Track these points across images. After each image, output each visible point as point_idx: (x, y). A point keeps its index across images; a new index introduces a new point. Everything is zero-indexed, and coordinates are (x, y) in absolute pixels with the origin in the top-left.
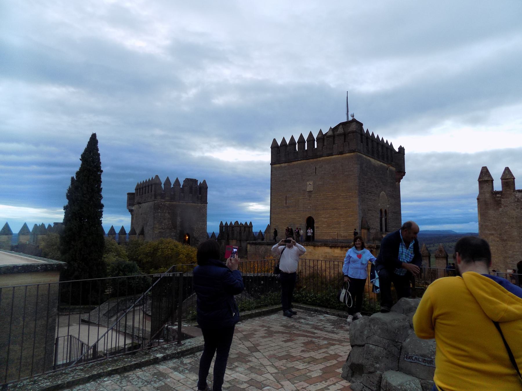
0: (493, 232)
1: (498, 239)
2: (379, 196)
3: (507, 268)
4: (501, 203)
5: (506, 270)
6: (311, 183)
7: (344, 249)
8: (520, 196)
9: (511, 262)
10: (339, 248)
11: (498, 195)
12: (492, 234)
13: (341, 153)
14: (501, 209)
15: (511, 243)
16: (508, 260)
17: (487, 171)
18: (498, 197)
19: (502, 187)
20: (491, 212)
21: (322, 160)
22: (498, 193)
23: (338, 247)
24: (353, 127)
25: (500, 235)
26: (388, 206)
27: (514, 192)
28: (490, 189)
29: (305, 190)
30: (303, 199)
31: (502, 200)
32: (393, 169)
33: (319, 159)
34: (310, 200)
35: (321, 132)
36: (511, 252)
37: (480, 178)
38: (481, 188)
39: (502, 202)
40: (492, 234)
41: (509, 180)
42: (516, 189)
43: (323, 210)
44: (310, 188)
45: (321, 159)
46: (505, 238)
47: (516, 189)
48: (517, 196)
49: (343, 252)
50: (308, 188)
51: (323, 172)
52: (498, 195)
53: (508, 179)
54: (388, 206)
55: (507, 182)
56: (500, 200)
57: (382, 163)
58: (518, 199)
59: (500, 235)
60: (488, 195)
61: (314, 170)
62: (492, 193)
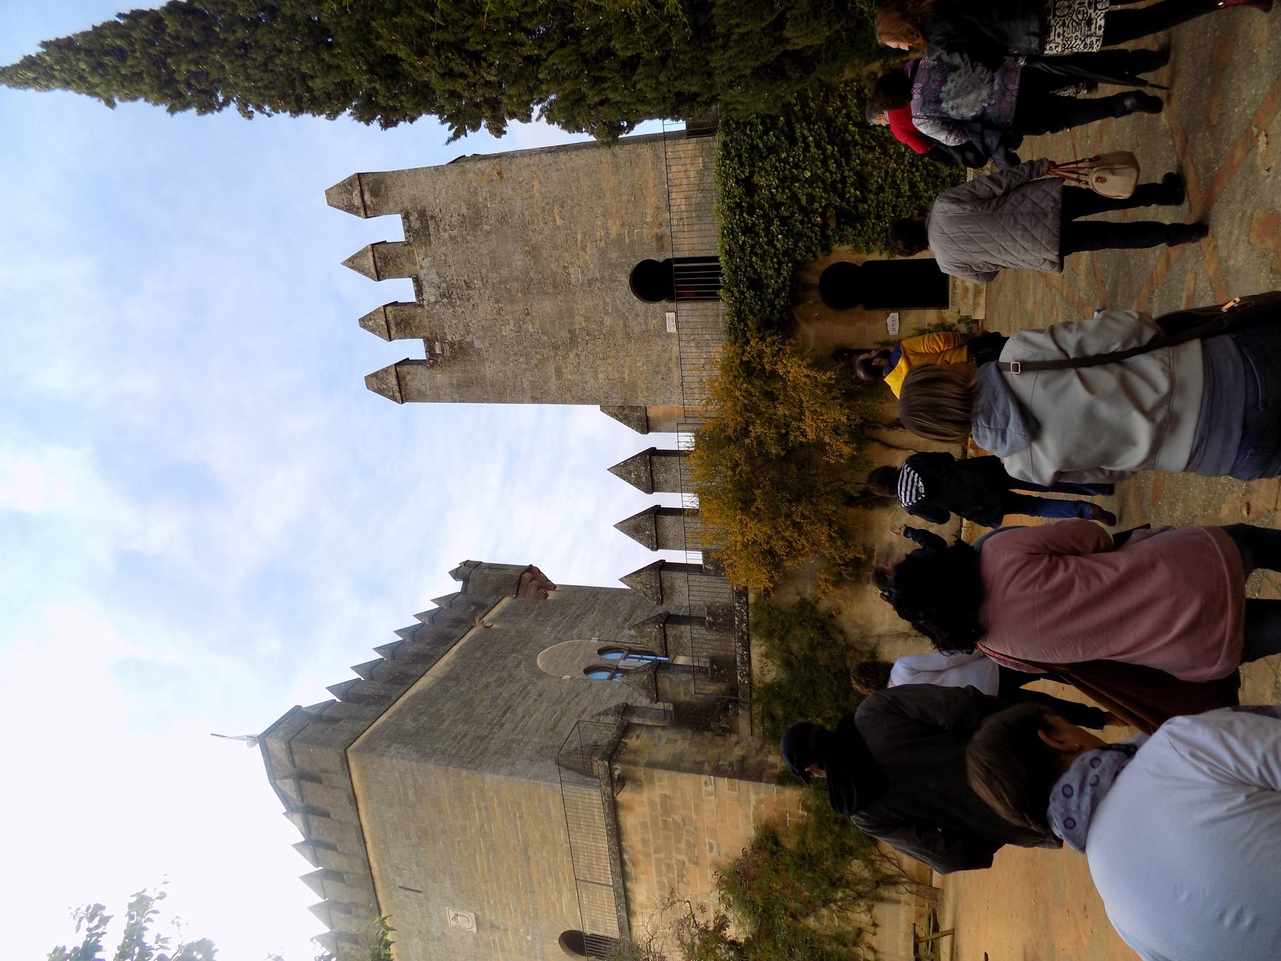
0: (551, 369)
1: (571, 355)
2: (541, 675)
3: (661, 332)
4: (459, 342)
5: (669, 335)
6: (452, 915)
7: (630, 868)
8: (433, 291)
9: (641, 319)
10: (629, 885)
11: (438, 351)
12: (559, 371)
13: (354, 800)
14: (478, 344)
15: (578, 319)
16: (636, 328)
17: (375, 375)
18: (443, 350)
19: (413, 337)
20: (489, 371)
21: (378, 862)
22: (430, 350)
23: (626, 890)
24: (277, 746)
25: (556, 348)
26: (594, 640)
27: (421, 306)
28: (421, 369)
29: (476, 939)
30: (503, 950)
31: (449, 338)
32: (506, 601)
33: (375, 872)
34: (506, 930)
35: (296, 846)
36: (608, 321)
37: (393, 398)
38: (421, 397)
39: (457, 338)
40: (559, 371)
41: (390, 318)
42: (413, 299)
43: (532, 892)
44: (466, 922)
45: (374, 864)
46: (564, 334)
47: (413, 299)
48: (433, 299)
49: (643, 877)
50: (466, 926)
51: (415, 869)
52: (438, 351)
53: (387, 322)
54: (594, 640)
55: (397, 324)
56: (452, 344)
57: (455, 648)
58: (443, 295)
59: (556, 348)
60: (441, 378)
61: (412, 894)
62: (432, 366)
